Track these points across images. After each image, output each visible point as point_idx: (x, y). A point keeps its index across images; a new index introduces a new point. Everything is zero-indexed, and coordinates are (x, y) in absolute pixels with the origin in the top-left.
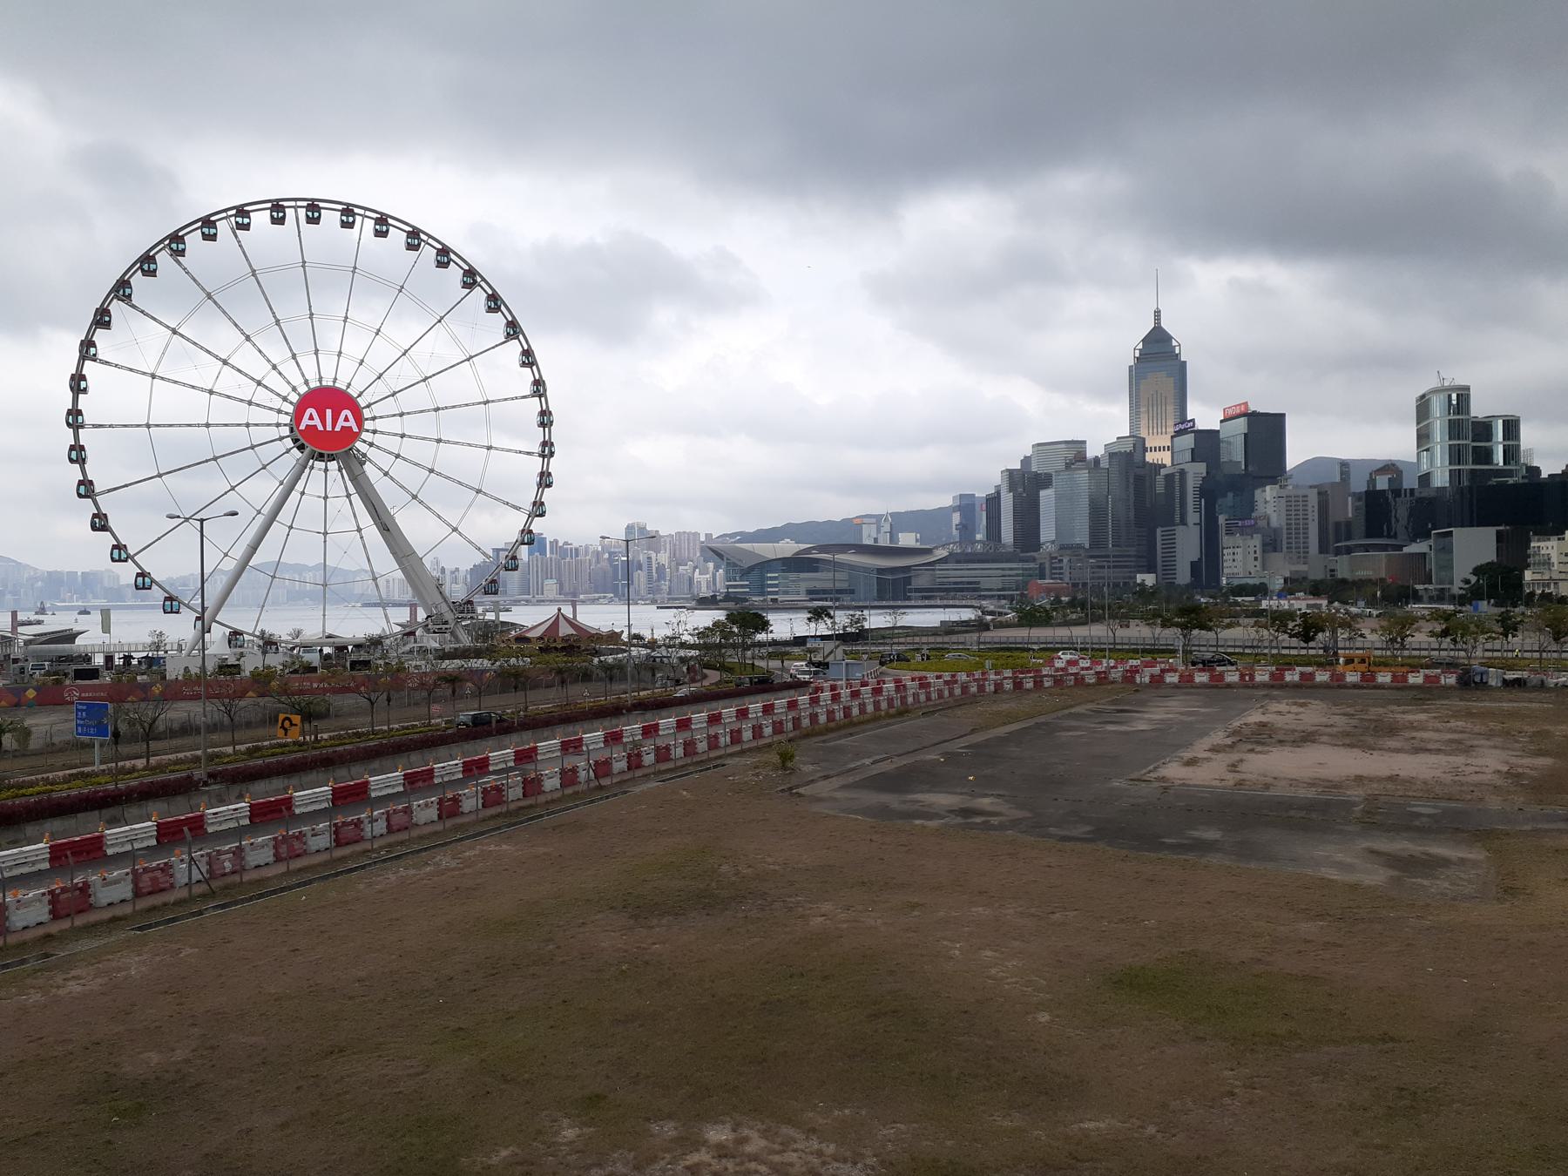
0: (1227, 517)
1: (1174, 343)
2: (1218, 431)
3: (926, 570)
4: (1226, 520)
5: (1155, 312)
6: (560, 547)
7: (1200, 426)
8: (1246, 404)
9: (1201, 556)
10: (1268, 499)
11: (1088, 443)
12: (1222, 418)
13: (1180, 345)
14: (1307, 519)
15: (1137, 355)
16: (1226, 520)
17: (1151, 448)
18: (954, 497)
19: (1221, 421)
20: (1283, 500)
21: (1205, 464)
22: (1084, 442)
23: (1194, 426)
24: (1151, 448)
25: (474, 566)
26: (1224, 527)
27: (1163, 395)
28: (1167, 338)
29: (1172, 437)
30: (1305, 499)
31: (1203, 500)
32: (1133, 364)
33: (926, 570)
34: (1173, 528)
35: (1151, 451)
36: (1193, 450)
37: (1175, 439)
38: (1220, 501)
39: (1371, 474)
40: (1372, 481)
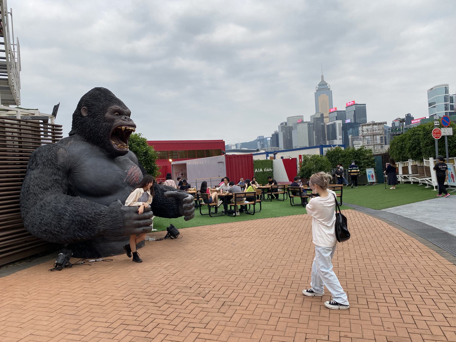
1: (328, 85)
2: (345, 111)
4: (351, 137)
5: (322, 76)
7: (338, 110)
8: (354, 101)
12: (346, 106)
13: (330, 86)
15: (317, 89)
16: (351, 137)
17: (325, 117)
18: (258, 137)
19: (346, 107)
24: (325, 117)
26: (350, 139)
28: (327, 84)
31: (343, 131)
32: (316, 92)
34: (334, 140)
35: (325, 118)
36: (336, 117)
38: (348, 131)
39: (393, 121)
40: (393, 124)
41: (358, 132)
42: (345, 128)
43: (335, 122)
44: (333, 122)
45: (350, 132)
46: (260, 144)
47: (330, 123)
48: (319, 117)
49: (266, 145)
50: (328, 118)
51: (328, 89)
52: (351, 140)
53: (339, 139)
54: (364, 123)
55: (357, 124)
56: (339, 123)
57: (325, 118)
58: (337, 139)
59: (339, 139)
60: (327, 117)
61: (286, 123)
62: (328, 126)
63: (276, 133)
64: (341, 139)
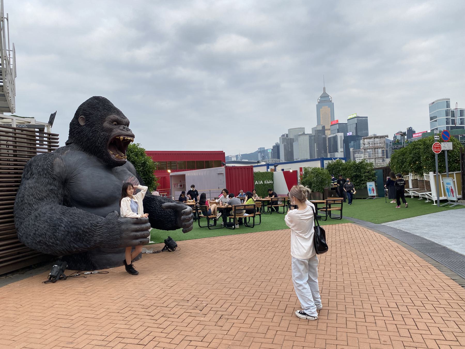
0: (353, 149)
1: (330, 97)
2: (347, 124)
4: (353, 150)
7: (340, 122)
11: (305, 128)
13: (332, 98)
15: (319, 101)
16: (353, 150)
17: (327, 129)
22: (304, 128)
24: (327, 129)
26: (352, 153)
27: (326, 112)
28: (328, 96)
31: (344, 144)
32: (317, 104)
35: (327, 130)
38: (350, 144)
39: (395, 135)
40: (395, 137)
41: (360, 145)
42: (347, 140)
45: (352, 145)
46: (261, 156)
47: (332, 136)
48: (320, 129)
49: (266, 157)
50: (329, 130)
51: (329, 101)
54: (366, 136)
55: (359, 136)
56: (340, 136)
57: (327, 130)
58: (338, 152)
60: (328, 129)
61: (287, 135)
62: (329, 138)
63: (277, 145)
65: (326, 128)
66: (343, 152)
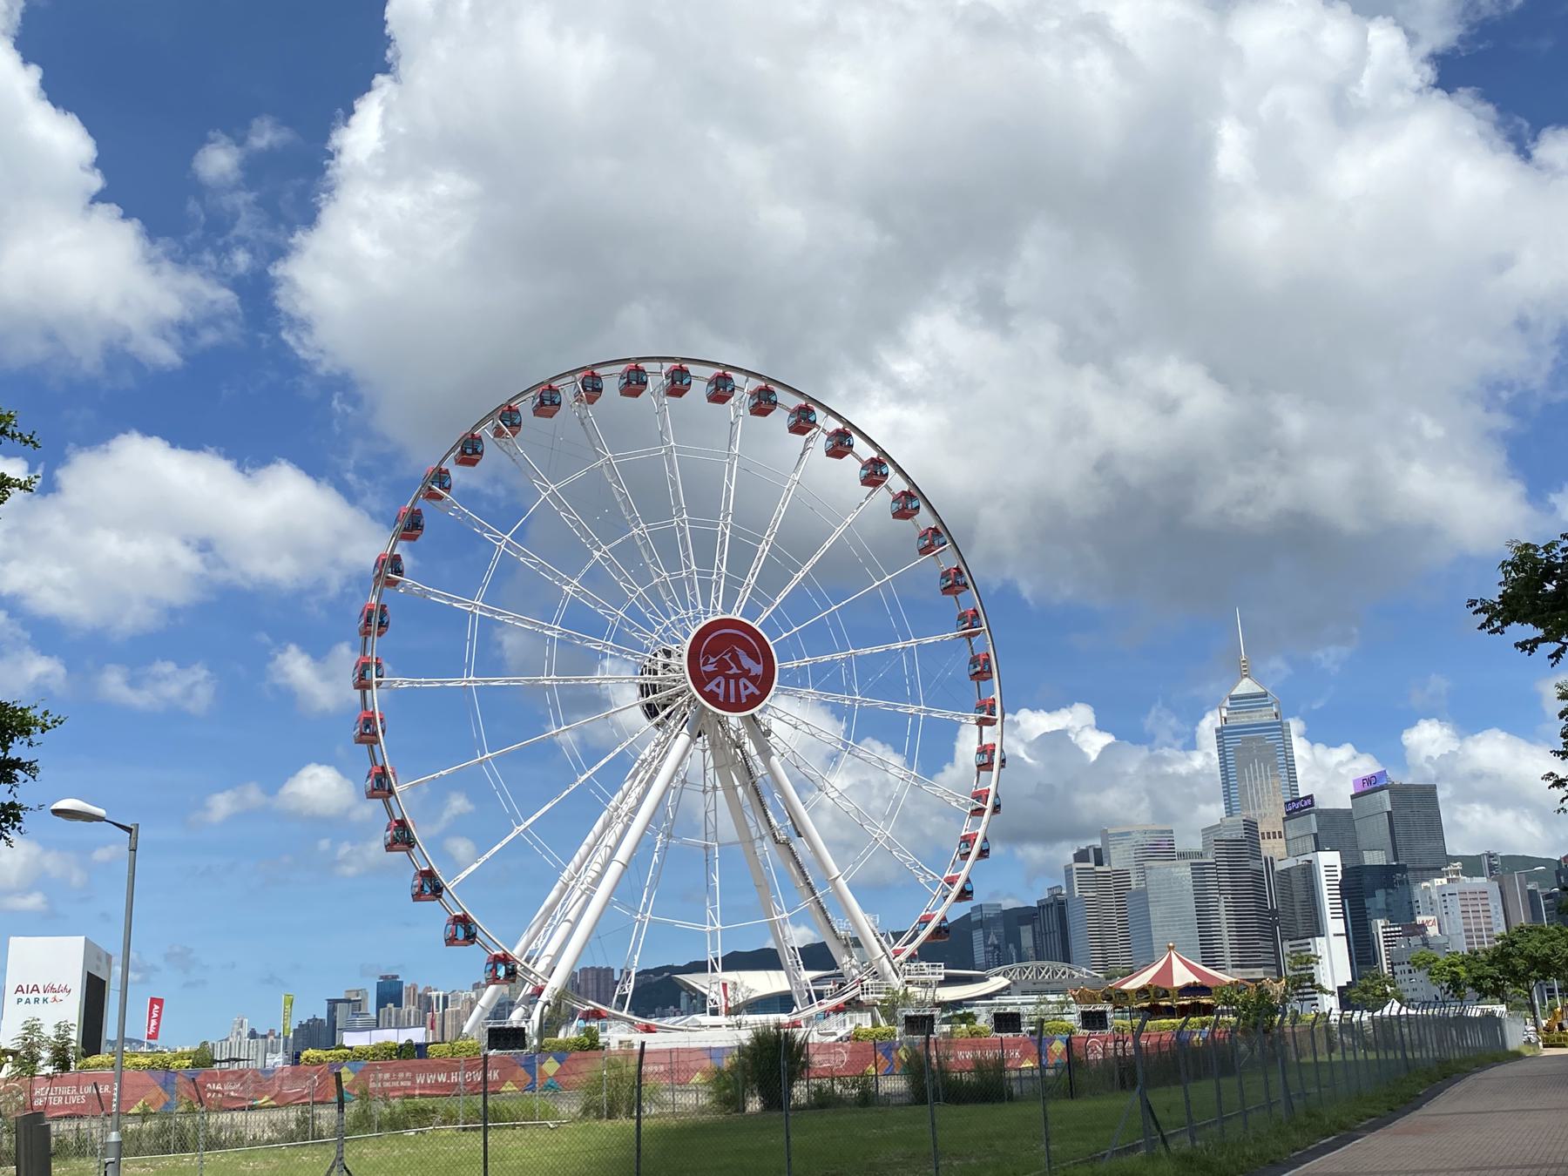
3: (983, 1005)
6: (420, 996)
7: (1323, 803)
9: (1353, 978)
10: (1435, 897)
12: (1353, 793)
14: (1490, 923)
16: (1383, 927)
19: (1353, 797)
20: (1458, 897)
21: (1338, 852)
23: (1312, 805)
25: (301, 1025)
26: (1381, 940)
29: (1285, 820)
30: (1484, 896)
31: (1346, 901)
33: (983, 1005)
34: (1310, 940)
37: (1287, 823)
38: (1368, 903)
41: (1412, 908)
43: (1310, 861)
44: (1301, 858)
45: (1379, 907)
47: (1290, 863)
51: (1271, 715)
52: (1381, 940)
53: (1335, 935)
55: (1403, 869)
56: (1329, 861)
58: (1323, 936)
59: (1335, 935)
63: (1055, 899)
64: (1342, 935)
65: (1262, 829)
66: (1345, 937)
